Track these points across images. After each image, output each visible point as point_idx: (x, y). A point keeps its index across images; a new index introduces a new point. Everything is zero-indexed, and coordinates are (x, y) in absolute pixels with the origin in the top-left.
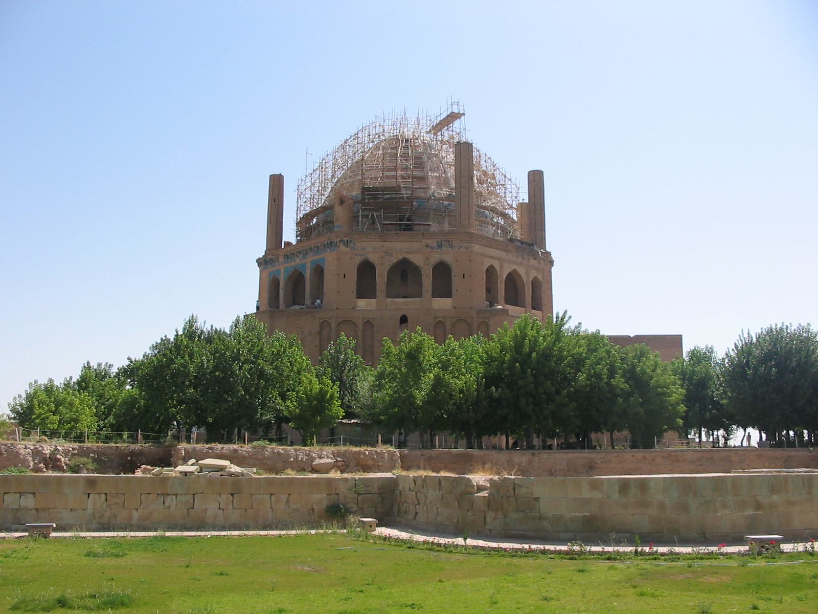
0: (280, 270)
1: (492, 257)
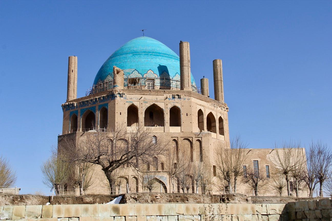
0: (78, 110)
1: (200, 105)
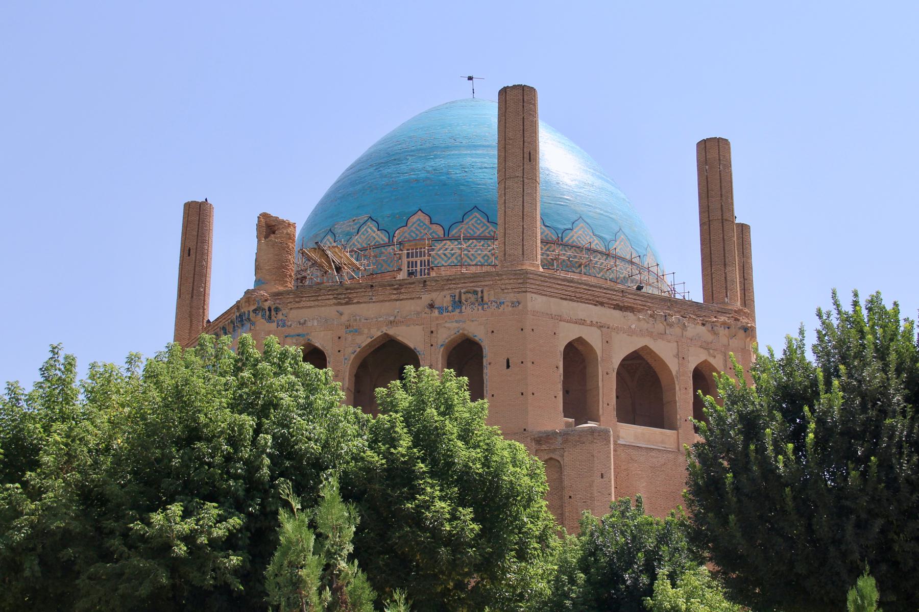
1: (582, 322)
